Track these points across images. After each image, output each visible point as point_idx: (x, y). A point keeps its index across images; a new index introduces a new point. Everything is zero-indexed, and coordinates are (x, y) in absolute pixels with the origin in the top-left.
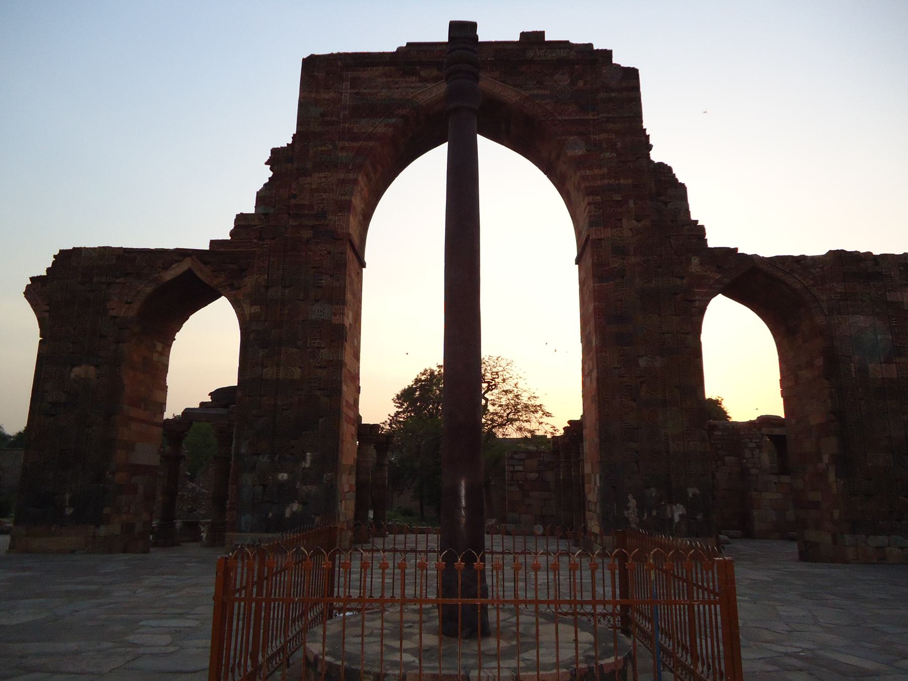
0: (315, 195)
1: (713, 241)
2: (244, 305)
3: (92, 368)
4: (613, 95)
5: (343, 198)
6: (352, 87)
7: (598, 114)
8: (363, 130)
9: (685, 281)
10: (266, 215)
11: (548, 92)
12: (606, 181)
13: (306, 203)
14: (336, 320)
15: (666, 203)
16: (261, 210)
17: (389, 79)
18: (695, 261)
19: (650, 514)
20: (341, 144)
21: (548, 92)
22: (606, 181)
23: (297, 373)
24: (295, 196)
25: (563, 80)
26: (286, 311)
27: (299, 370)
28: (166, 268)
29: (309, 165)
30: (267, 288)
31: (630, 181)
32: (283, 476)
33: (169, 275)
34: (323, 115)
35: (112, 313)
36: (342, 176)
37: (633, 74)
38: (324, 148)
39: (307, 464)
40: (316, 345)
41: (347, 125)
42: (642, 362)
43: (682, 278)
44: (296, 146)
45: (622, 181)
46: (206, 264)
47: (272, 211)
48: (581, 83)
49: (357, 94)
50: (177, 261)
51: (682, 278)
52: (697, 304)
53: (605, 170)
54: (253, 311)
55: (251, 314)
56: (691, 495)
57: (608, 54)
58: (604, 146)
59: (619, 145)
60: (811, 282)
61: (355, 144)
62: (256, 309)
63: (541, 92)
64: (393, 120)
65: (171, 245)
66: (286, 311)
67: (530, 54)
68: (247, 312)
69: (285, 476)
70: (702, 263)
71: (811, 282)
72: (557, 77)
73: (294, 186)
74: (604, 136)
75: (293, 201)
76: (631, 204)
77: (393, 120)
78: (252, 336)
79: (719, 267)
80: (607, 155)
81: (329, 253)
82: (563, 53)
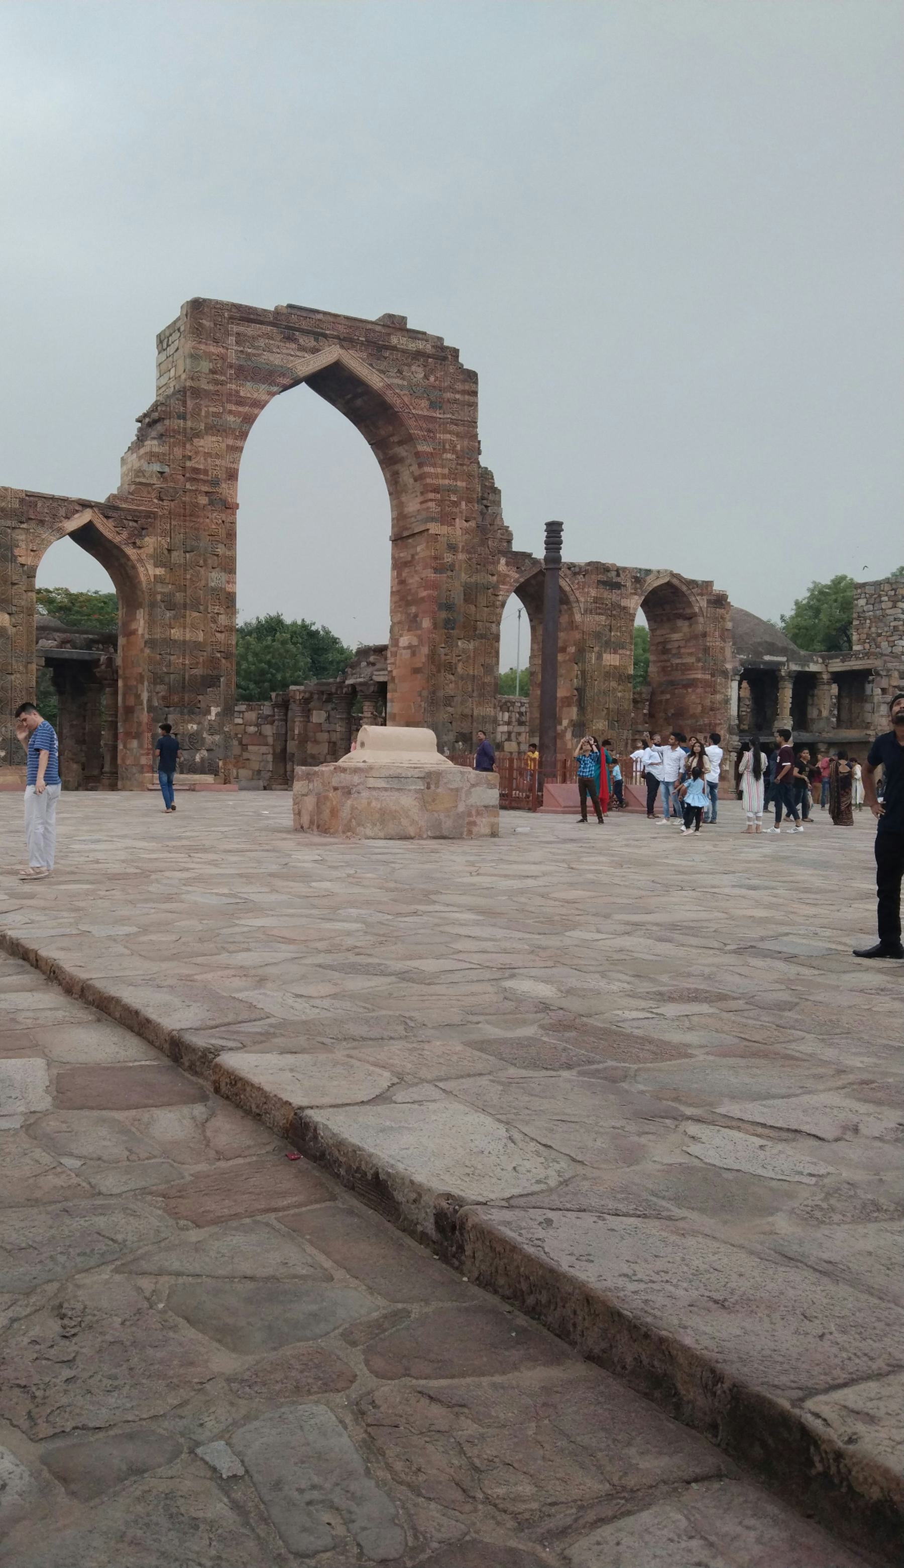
0: (209, 460)
1: (517, 547)
2: (148, 567)
3: (7, 616)
4: (458, 396)
7: (444, 413)
8: (249, 395)
9: (495, 578)
10: (162, 473)
11: (405, 383)
12: (447, 482)
13: (202, 467)
16: (156, 467)
17: (272, 342)
18: (503, 561)
21: (405, 383)
22: (447, 482)
24: (190, 458)
25: (417, 373)
28: (67, 518)
30: (169, 551)
31: (464, 484)
32: (193, 727)
34: (213, 372)
35: (21, 560)
36: (230, 442)
37: (472, 377)
38: (215, 410)
39: (212, 717)
40: (216, 611)
41: (234, 387)
44: (189, 402)
45: (459, 483)
46: (107, 517)
47: (167, 469)
48: (432, 379)
49: (241, 351)
50: (77, 511)
51: (493, 575)
52: (500, 598)
53: (446, 471)
54: (158, 573)
55: (155, 576)
57: (455, 352)
58: (447, 447)
59: (459, 447)
60: (577, 586)
61: (241, 409)
62: (159, 571)
63: (400, 382)
65: (75, 494)
66: (188, 577)
67: (394, 340)
68: (151, 572)
69: (195, 727)
70: (507, 564)
71: (577, 586)
72: (414, 368)
73: (188, 446)
74: (448, 436)
76: (463, 503)
78: (159, 597)
80: (449, 456)
82: (420, 345)
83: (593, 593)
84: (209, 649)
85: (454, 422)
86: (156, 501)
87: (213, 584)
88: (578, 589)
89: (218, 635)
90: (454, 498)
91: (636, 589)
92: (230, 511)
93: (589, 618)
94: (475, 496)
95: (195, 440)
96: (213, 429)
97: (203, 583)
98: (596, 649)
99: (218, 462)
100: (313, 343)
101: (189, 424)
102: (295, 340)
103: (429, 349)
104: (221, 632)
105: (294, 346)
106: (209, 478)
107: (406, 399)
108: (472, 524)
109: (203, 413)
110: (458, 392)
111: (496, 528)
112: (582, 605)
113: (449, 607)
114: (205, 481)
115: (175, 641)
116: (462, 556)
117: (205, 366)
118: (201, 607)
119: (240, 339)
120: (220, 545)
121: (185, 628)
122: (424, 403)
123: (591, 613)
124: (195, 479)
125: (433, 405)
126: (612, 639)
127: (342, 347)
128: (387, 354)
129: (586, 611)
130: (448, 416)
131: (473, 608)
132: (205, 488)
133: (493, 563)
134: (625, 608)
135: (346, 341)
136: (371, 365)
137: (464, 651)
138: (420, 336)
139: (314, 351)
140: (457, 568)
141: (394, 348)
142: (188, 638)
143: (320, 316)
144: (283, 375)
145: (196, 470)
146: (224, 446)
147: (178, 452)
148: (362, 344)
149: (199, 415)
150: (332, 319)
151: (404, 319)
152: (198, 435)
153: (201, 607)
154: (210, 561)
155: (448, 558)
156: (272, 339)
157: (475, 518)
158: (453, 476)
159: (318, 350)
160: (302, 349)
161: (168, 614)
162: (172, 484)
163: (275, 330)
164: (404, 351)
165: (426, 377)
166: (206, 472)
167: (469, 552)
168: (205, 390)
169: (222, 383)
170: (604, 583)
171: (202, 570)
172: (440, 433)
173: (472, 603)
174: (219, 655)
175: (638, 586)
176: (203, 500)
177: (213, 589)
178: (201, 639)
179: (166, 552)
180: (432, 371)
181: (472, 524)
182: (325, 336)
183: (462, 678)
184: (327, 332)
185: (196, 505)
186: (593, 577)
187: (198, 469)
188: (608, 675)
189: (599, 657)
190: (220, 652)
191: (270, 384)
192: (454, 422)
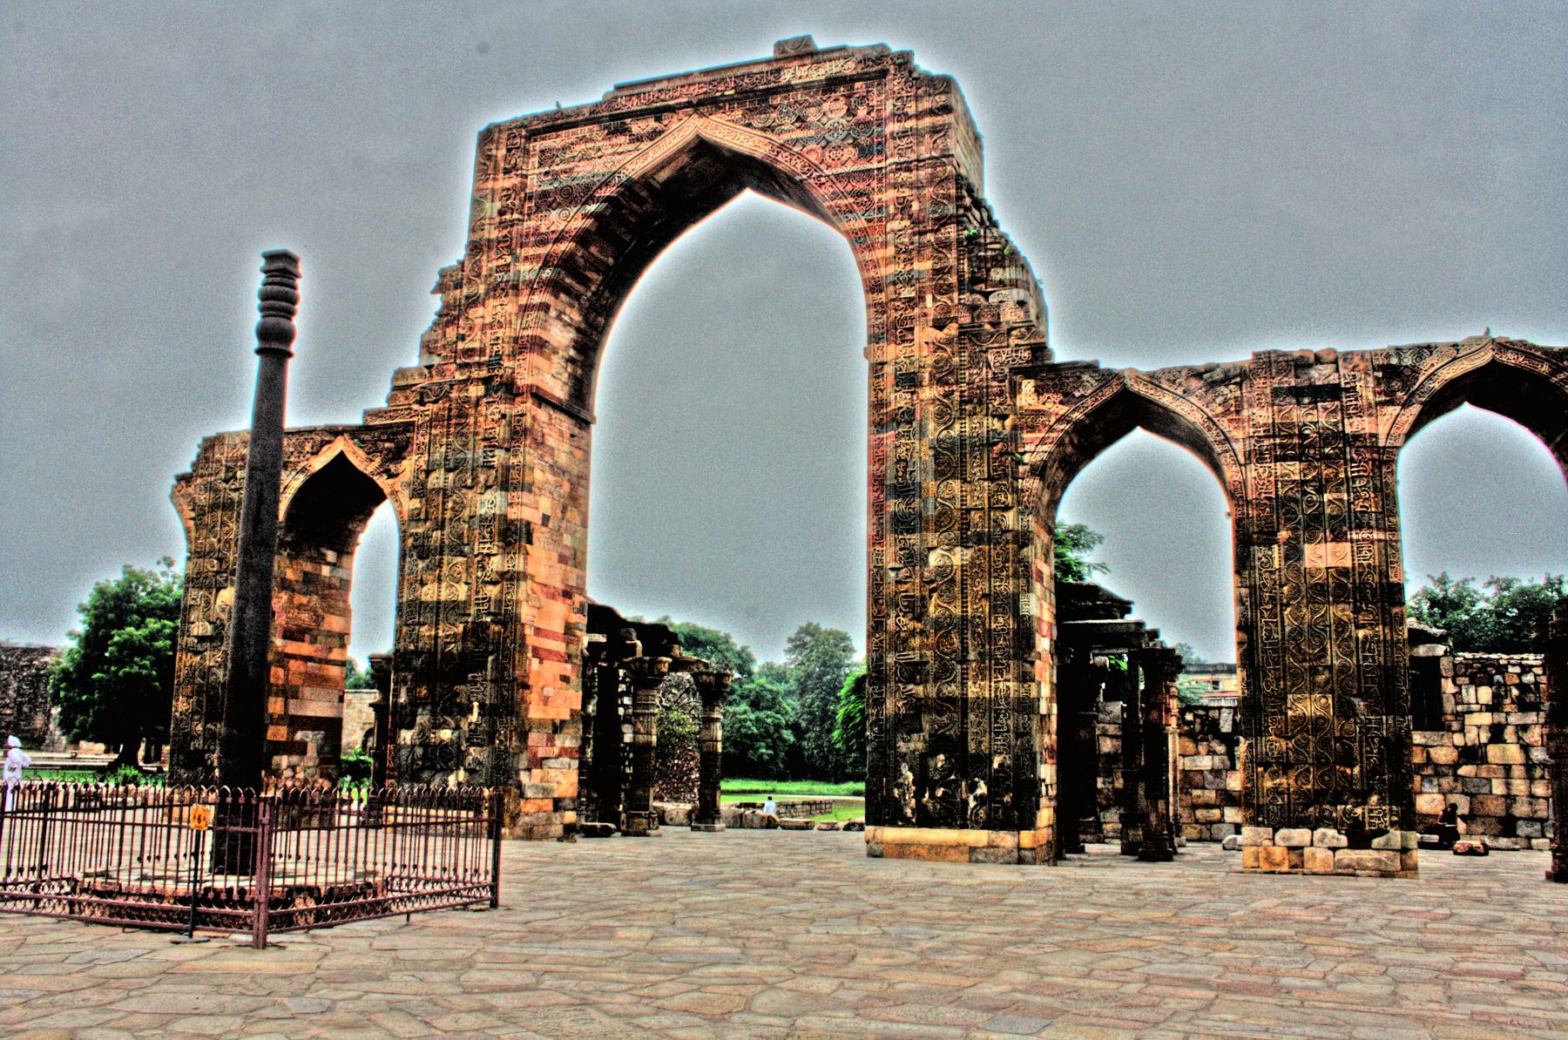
4: (910, 124)
5: (525, 333)
6: (541, 165)
10: (429, 367)
11: (812, 133)
12: (892, 269)
13: (477, 345)
14: (513, 514)
15: (986, 295)
18: (1028, 386)
19: (932, 796)
20: (523, 252)
22: (892, 269)
23: (462, 592)
24: (463, 338)
26: (450, 505)
27: (465, 588)
28: (315, 453)
29: (482, 289)
30: (428, 473)
32: (446, 735)
33: (318, 463)
34: (501, 213)
36: (523, 300)
42: (934, 559)
43: (1003, 417)
45: (917, 266)
48: (862, 113)
49: (547, 173)
51: (1003, 417)
53: (891, 251)
56: (996, 765)
59: (915, 206)
60: (1220, 410)
62: (416, 503)
64: (592, 208)
66: (450, 505)
67: (786, 77)
70: (1039, 391)
71: (1220, 410)
72: (826, 106)
74: (891, 194)
75: (461, 345)
76: (929, 298)
77: (592, 208)
78: (410, 541)
79: (1065, 395)
80: (895, 225)
81: (504, 416)
83: (1263, 415)
84: (473, 610)
85: (900, 167)
86: (415, 407)
87: (482, 512)
88: (1224, 414)
89: (490, 588)
90: (908, 292)
91: (1390, 393)
92: (519, 399)
93: (1252, 472)
94: (953, 279)
95: (472, 313)
96: (495, 290)
97: (466, 513)
98: (1283, 534)
99: (500, 333)
100: (651, 124)
101: (465, 291)
102: (623, 130)
103: (850, 68)
104: (494, 583)
105: (622, 139)
106: (486, 358)
107: (813, 158)
108: (952, 330)
109: (484, 272)
110: (908, 117)
111: (1004, 327)
112: (1238, 447)
113: (904, 490)
114: (479, 365)
115: (427, 603)
116: (928, 393)
117: (492, 208)
118: (466, 549)
119: (546, 157)
120: (497, 452)
121: (440, 581)
122: (849, 153)
123: (1260, 460)
124: (467, 365)
125: (865, 153)
126: (1328, 511)
127: (702, 115)
128: (777, 100)
129: (1248, 455)
130: (891, 160)
131: (956, 485)
132: (484, 373)
133: (1001, 394)
134: (1356, 437)
135: (707, 104)
136: (749, 125)
137: (942, 571)
138: (836, 55)
139: (654, 135)
140: (918, 417)
141: (788, 88)
142: (445, 595)
143: (664, 85)
144: (606, 184)
145: (469, 352)
146: (511, 308)
147: (451, 333)
148: (731, 100)
149: (478, 276)
150: (684, 82)
151: (806, 41)
152: (473, 301)
153: (466, 549)
154: (482, 478)
155: (898, 400)
156: (592, 140)
157: (955, 319)
158: (903, 256)
159: (661, 132)
160: (639, 139)
161: (421, 565)
162: (436, 379)
163: (596, 128)
164: (807, 87)
165: (851, 113)
166: (482, 352)
167: (941, 382)
168: (489, 240)
169: (512, 223)
170: (1297, 393)
171: (470, 494)
172: (880, 191)
173: (953, 477)
174: (489, 619)
175: (1396, 385)
176: (475, 391)
177: (483, 519)
178: (462, 597)
179: (422, 476)
180: (863, 99)
181: (952, 330)
182: (672, 109)
183: (938, 624)
184: (672, 103)
185: (467, 400)
186: (1259, 382)
187: (472, 350)
188: (1319, 592)
189: (1293, 552)
190: (489, 614)
191: (586, 203)
192: (900, 167)
